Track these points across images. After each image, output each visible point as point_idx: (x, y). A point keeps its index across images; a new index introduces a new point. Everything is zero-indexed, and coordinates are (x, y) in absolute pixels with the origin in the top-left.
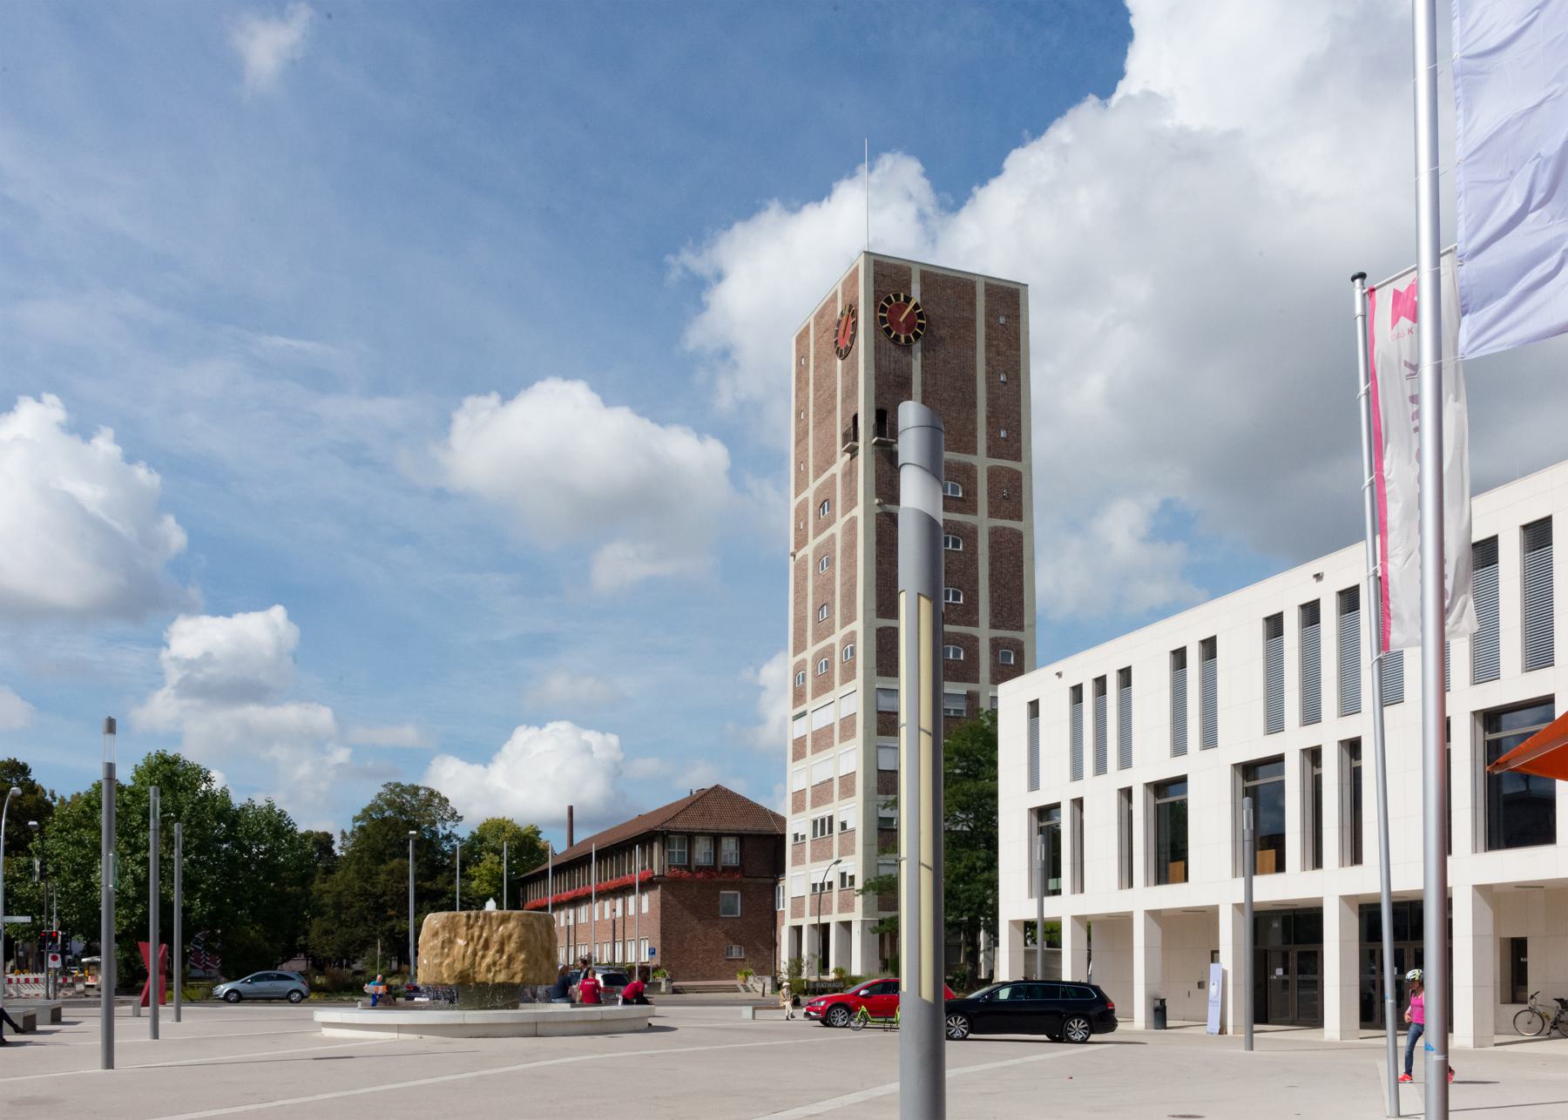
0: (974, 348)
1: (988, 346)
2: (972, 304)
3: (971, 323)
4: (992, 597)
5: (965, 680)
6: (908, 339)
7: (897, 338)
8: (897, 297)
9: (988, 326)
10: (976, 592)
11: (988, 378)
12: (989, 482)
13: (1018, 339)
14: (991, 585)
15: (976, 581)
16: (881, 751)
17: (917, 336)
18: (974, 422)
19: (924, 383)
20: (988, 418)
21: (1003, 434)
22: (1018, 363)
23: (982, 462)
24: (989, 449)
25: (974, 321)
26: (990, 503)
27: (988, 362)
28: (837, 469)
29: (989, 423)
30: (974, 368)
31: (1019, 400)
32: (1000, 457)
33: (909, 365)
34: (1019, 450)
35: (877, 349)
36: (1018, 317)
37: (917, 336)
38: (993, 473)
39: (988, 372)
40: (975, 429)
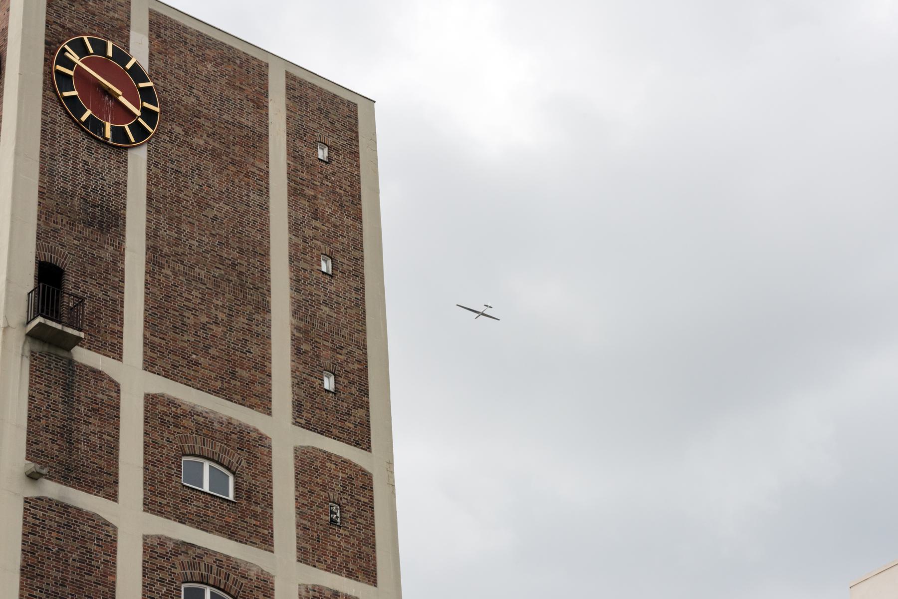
0: (264, 191)
1: (295, 192)
2: (260, 104)
3: (258, 140)
6: (119, 133)
7: (95, 125)
8: (100, 47)
9: (294, 154)
11: (293, 259)
12: (300, 483)
13: (356, 199)
17: (140, 133)
18: (265, 339)
19: (152, 235)
20: (296, 343)
21: (329, 383)
22: (358, 244)
23: (283, 434)
24: (298, 406)
25: (263, 137)
27: (295, 227)
29: (297, 352)
30: (264, 229)
31: (361, 318)
32: (325, 431)
33: (120, 186)
34: (365, 425)
35: (47, 135)
36: (355, 154)
37: (140, 133)
38: (308, 465)
39: (293, 246)
40: (266, 358)
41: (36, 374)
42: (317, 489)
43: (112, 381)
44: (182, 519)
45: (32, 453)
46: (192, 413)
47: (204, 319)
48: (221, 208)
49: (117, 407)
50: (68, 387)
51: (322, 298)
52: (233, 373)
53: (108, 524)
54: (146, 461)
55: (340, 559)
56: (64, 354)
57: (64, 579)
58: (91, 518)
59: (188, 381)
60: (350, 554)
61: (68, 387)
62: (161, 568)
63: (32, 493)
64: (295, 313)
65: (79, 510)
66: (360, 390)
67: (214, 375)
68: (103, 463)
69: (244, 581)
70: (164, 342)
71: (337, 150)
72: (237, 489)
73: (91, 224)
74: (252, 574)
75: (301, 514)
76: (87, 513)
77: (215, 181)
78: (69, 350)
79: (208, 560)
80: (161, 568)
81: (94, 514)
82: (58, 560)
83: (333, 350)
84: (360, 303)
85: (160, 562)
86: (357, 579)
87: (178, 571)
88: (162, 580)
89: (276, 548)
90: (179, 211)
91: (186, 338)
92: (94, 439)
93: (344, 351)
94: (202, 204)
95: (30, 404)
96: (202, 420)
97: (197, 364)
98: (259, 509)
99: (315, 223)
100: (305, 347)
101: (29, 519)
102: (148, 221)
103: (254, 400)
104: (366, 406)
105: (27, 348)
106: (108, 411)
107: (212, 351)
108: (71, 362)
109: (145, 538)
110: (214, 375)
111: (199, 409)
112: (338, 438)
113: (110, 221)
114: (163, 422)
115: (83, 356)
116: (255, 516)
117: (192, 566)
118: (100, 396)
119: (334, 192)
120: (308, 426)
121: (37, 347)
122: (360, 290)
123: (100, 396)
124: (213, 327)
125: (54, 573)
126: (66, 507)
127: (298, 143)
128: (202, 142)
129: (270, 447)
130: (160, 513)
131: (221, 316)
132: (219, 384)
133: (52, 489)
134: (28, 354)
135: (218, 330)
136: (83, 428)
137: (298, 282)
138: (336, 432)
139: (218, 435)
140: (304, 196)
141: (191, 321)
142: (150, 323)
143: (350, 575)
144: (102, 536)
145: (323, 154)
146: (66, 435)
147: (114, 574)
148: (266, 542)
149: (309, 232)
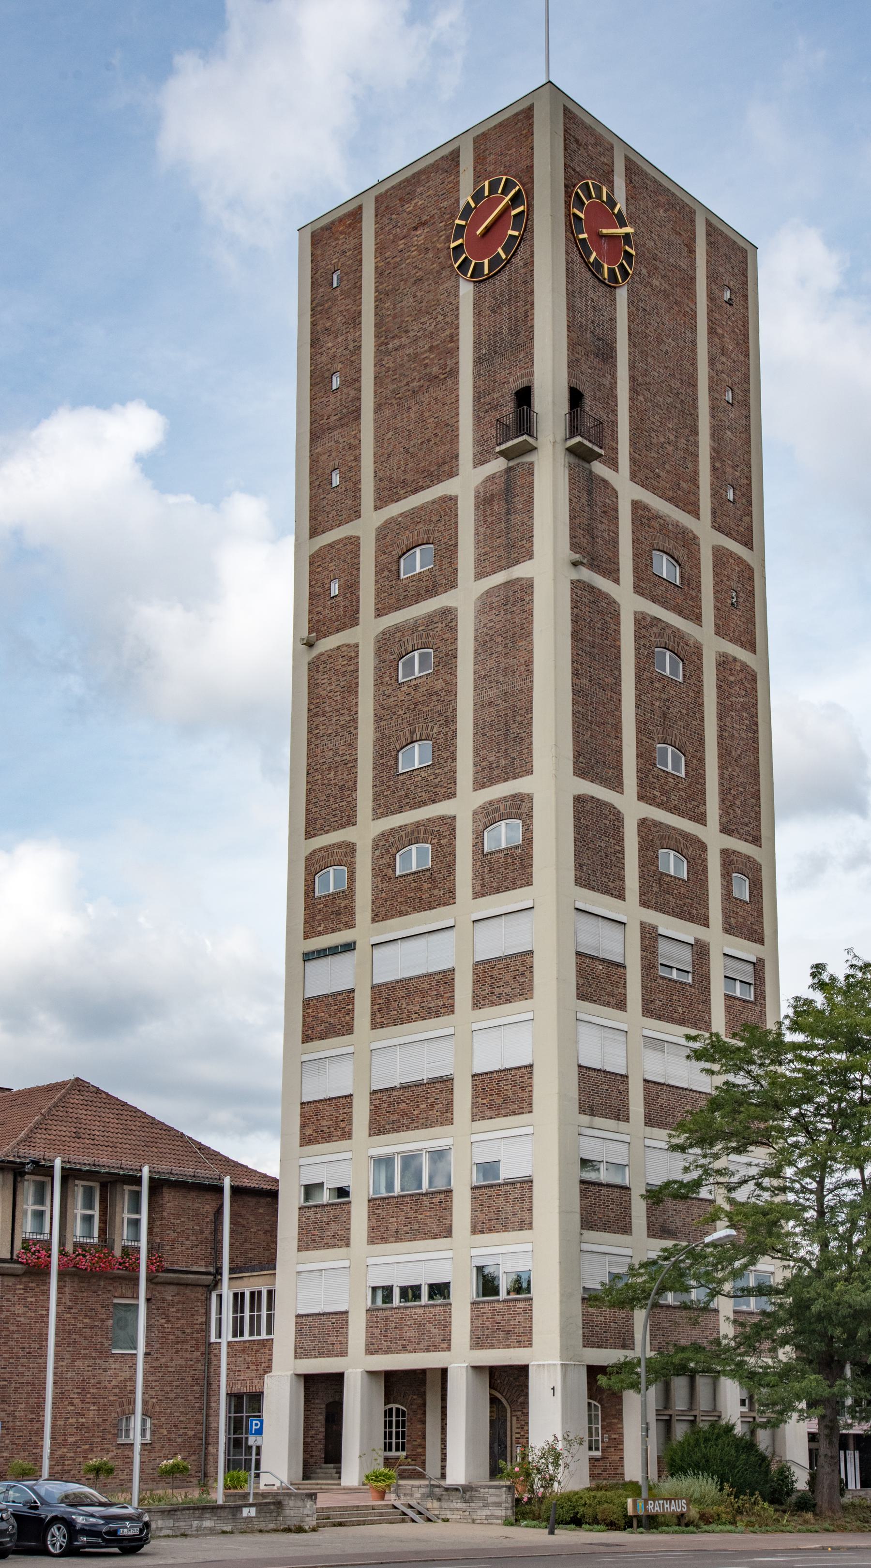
0: (694, 329)
1: (712, 331)
4: (721, 776)
5: (691, 919)
9: (712, 298)
10: (702, 760)
11: (711, 389)
12: (716, 574)
14: (721, 756)
15: (702, 741)
16: (583, 1028)
18: (695, 456)
19: (632, 367)
25: (693, 279)
26: (717, 609)
28: (467, 482)
29: (714, 469)
34: (750, 529)
39: (711, 378)
40: (696, 472)
41: (573, 481)
42: (724, 579)
43: (613, 489)
44: (654, 600)
45: (575, 546)
46: (658, 517)
47: (662, 440)
48: (669, 344)
49: (616, 510)
50: (590, 493)
51: (727, 424)
52: (679, 484)
53: (615, 602)
54: (634, 554)
55: (737, 634)
56: (586, 465)
57: (594, 642)
58: (606, 596)
59: (654, 490)
60: (742, 630)
61: (590, 493)
62: (644, 637)
63: (575, 576)
64: (712, 436)
65: (600, 590)
66: (748, 501)
67: (668, 486)
68: (610, 554)
69: (687, 648)
70: (640, 458)
71: (736, 293)
72: (682, 577)
73: (597, 356)
74: (691, 642)
75: (716, 599)
76: (604, 593)
77: (666, 318)
78: (589, 462)
79: (668, 631)
80: (644, 637)
81: (607, 594)
82: (590, 628)
83: (733, 468)
84: (747, 429)
85: (643, 631)
86: (745, 648)
87: (652, 639)
88: (644, 645)
89: (703, 624)
90: (647, 346)
91: (652, 455)
92: (605, 535)
93: (739, 469)
94: (659, 341)
95: (570, 505)
96: (662, 522)
97: (659, 477)
98: (694, 594)
99: (723, 359)
100: (718, 465)
101: (574, 596)
102: (630, 354)
103: (690, 507)
104: (750, 514)
105: (567, 460)
106: (611, 513)
107: (667, 467)
108: (591, 472)
109: (636, 613)
110: (668, 486)
111: (661, 514)
112: (735, 539)
113: (607, 355)
114: (642, 524)
115: (599, 468)
116: (692, 598)
117: (661, 635)
118: (607, 501)
119: (734, 332)
120: (719, 529)
121: (573, 460)
122: (748, 417)
123: (607, 501)
124: (667, 446)
125: (588, 638)
126: (593, 588)
127: (714, 287)
128: (658, 284)
129: (699, 545)
130: (642, 595)
131: (672, 437)
132: (671, 493)
133: (586, 574)
134: (567, 465)
135: (670, 448)
136: (599, 525)
137: (714, 409)
138: (734, 534)
139: (671, 535)
140: (717, 334)
141: (655, 441)
142: (633, 443)
143: (742, 646)
144: (612, 611)
145: (727, 295)
146: (590, 531)
147: (619, 640)
148: (697, 618)
149: (720, 367)
